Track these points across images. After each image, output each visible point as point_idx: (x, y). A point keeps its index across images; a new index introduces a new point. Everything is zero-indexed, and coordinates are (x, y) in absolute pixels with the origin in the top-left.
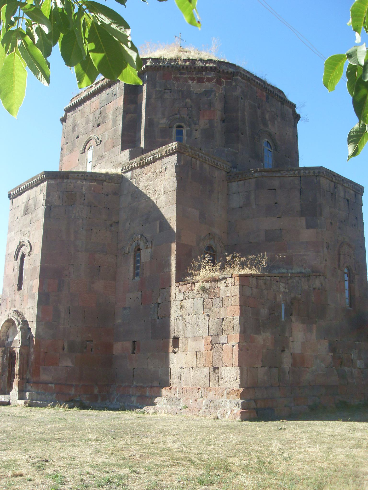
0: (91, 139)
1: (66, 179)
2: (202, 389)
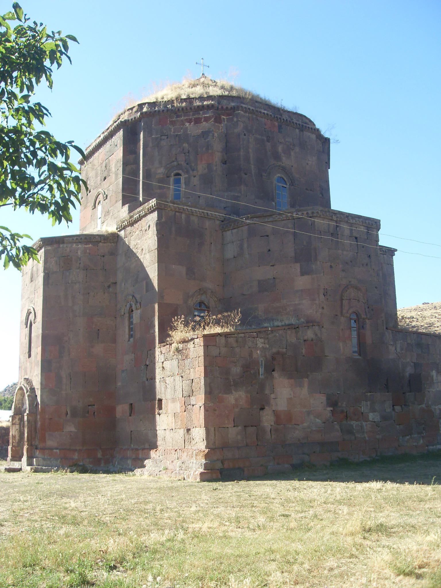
0: (100, 194)
2: (178, 450)
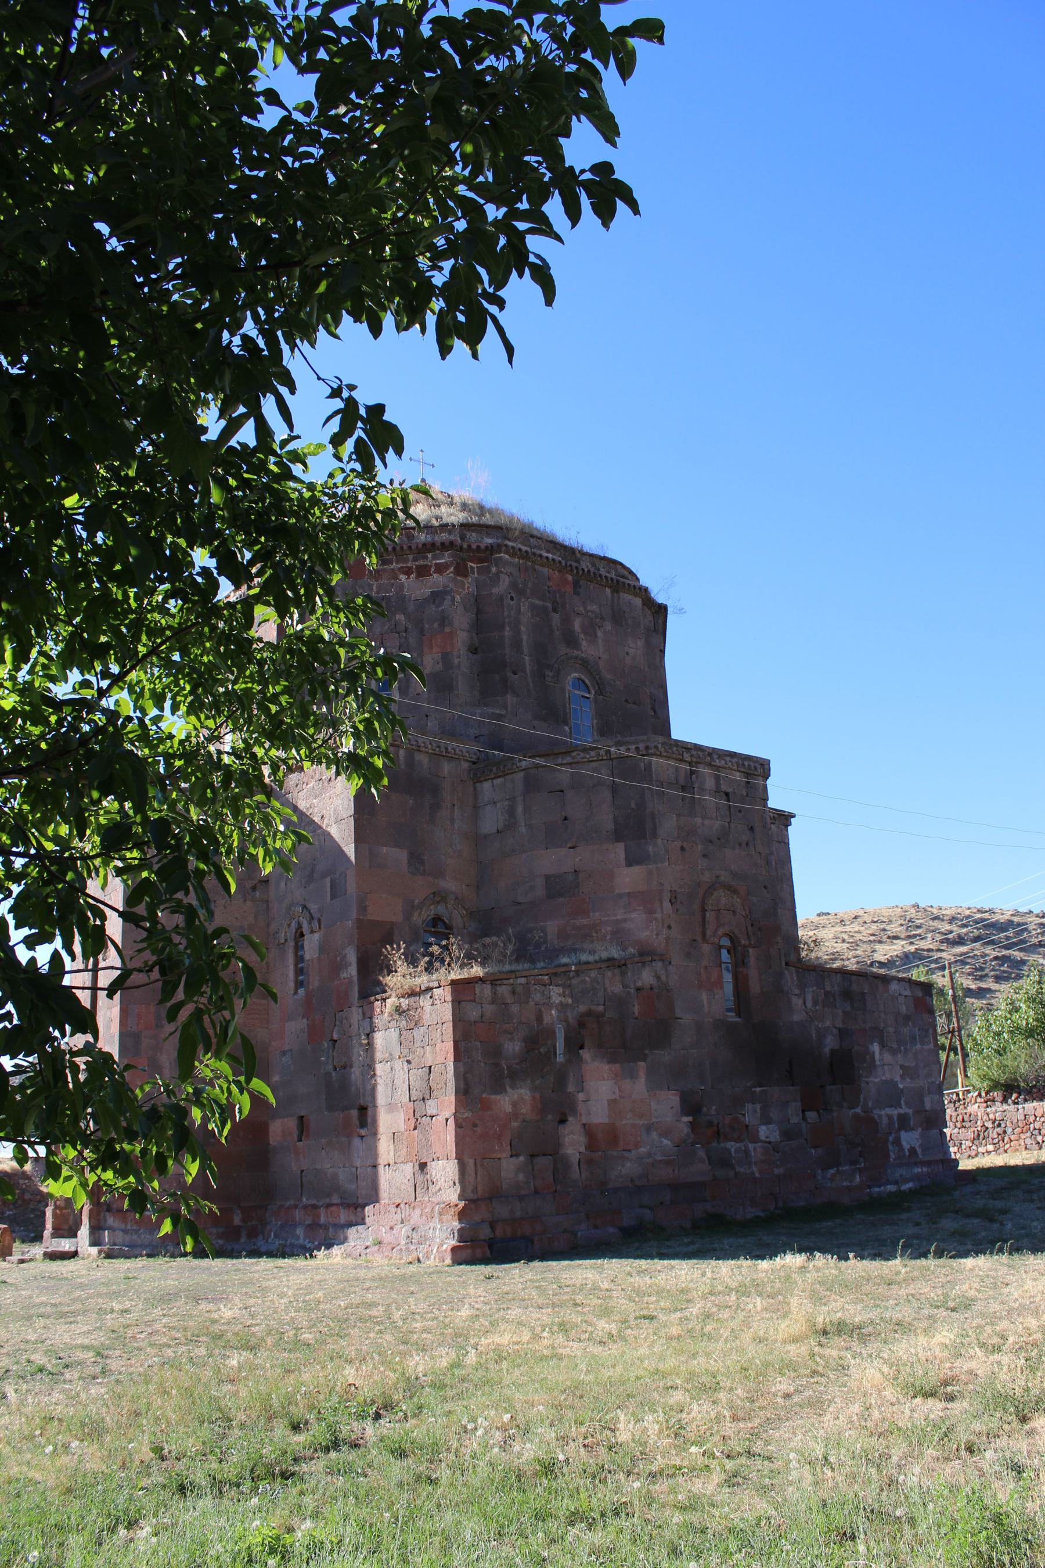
2: (402, 1205)
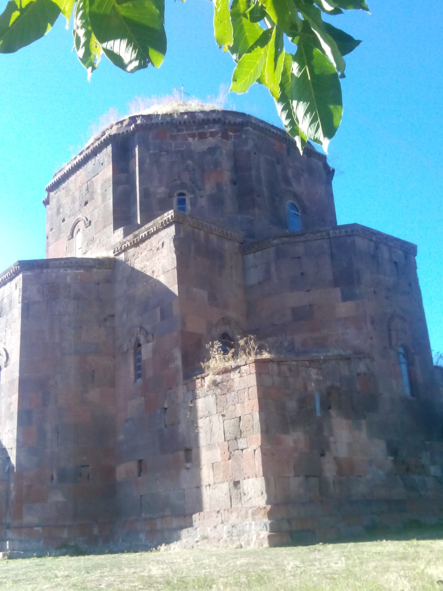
1: (45, 268)
